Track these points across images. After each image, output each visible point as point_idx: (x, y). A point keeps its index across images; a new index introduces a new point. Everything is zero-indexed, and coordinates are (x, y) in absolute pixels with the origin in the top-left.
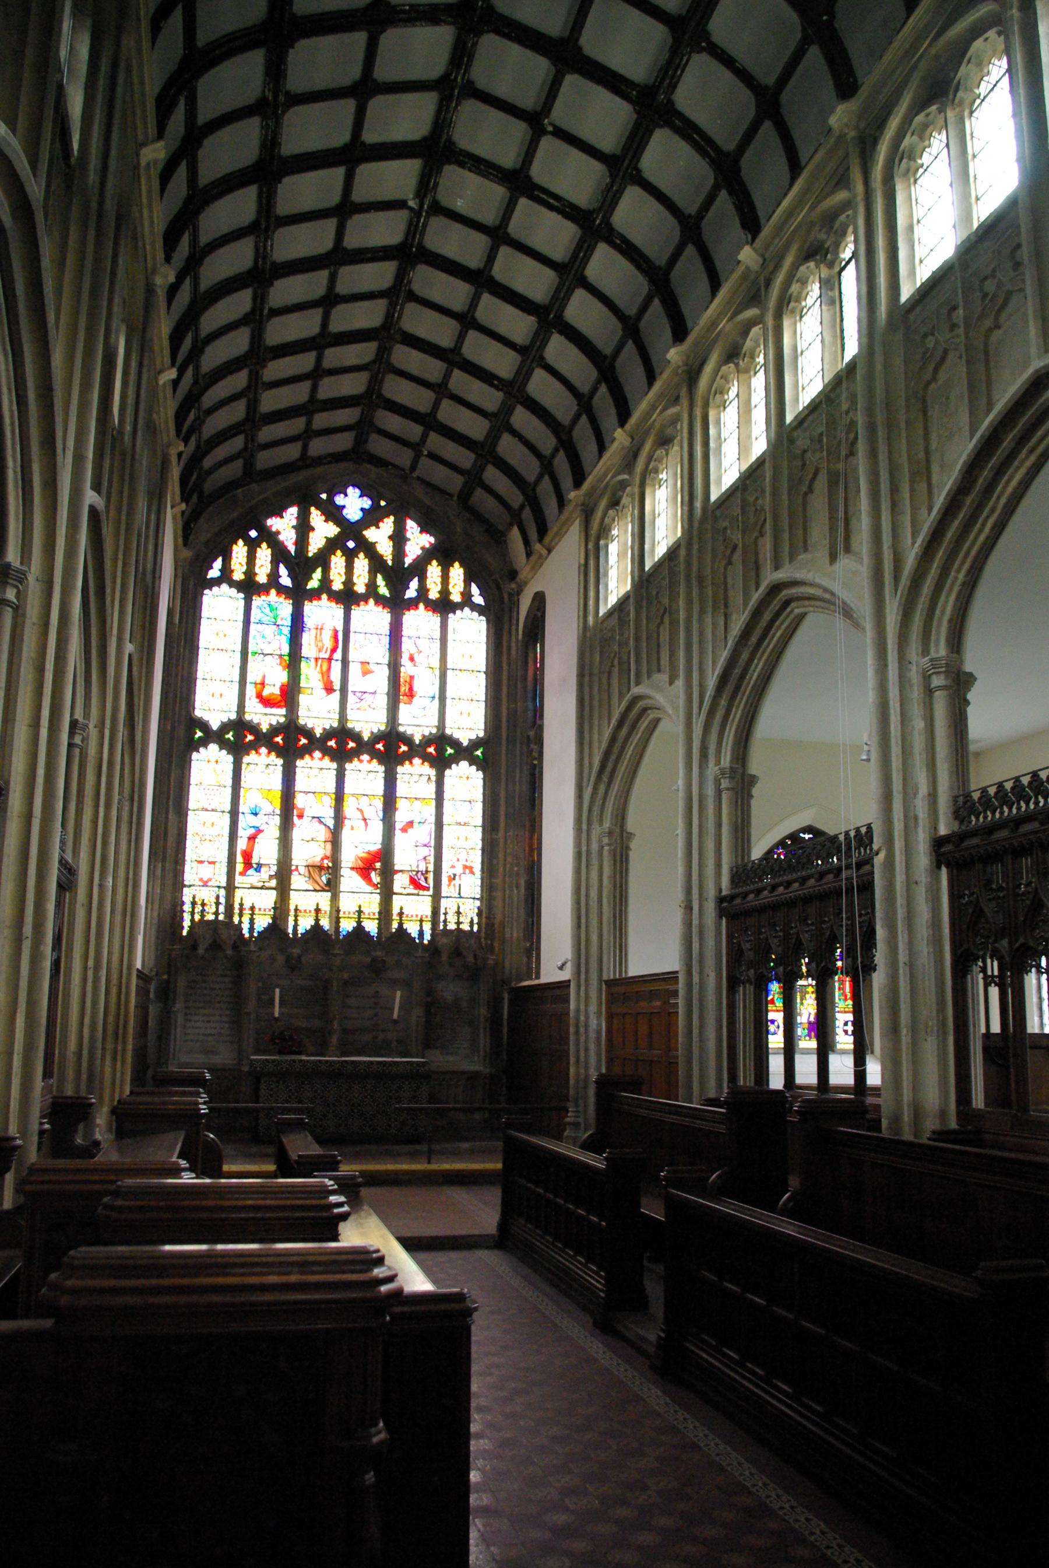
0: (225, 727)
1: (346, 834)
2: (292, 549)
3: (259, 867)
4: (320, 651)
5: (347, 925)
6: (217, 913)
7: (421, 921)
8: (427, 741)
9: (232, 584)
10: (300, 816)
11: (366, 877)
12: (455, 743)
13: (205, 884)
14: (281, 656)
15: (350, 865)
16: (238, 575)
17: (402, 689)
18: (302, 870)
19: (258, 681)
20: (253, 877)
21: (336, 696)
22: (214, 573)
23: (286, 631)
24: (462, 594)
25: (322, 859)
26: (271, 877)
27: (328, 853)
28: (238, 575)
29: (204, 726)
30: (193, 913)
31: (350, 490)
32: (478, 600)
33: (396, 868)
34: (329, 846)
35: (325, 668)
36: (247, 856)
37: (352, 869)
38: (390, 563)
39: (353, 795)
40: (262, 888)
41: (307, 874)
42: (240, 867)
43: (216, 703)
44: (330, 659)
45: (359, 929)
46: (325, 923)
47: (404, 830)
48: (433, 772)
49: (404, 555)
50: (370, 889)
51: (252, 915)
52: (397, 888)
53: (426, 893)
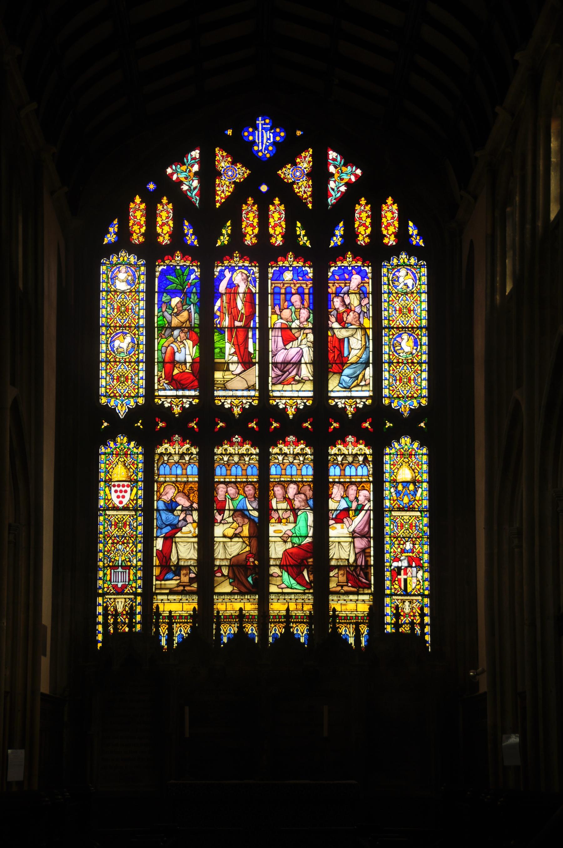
0: (133, 413)
1: (274, 529)
2: (196, 200)
3: (178, 569)
4: (233, 319)
5: (276, 630)
6: (131, 625)
7: (357, 624)
8: (362, 414)
9: (132, 249)
10: (222, 511)
11: (297, 576)
12: (395, 415)
13: (120, 592)
14: (191, 329)
15: (278, 563)
16: (137, 238)
17: (331, 356)
18: (225, 571)
19: (167, 359)
20: (172, 583)
21: (255, 371)
22: (110, 238)
23: (194, 298)
24: (396, 235)
25: (247, 558)
26: (191, 580)
27: (254, 551)
28: (137, 238)
29: (111, 413)
30: (105, 625)
31: (260, 122)
32: (418, 241)
33: (333, 563)
34: (254, 542)
35: (241, 339)
36: (165, 555)
37: (281, 567)
38: (310, 206)
39: (279, 483)
40: (183, 593)
41: (231, 575)
42: (156, 571)
43: (122, 389)
44: (246, 328)
45: (288, 635)
46: (251, 629)
47: (339, 520)
48: (368, 451)
49: (326, 194)
50: (299, 588)
51: (170, 624)
52: (333, 585)
53: (366, 591)
